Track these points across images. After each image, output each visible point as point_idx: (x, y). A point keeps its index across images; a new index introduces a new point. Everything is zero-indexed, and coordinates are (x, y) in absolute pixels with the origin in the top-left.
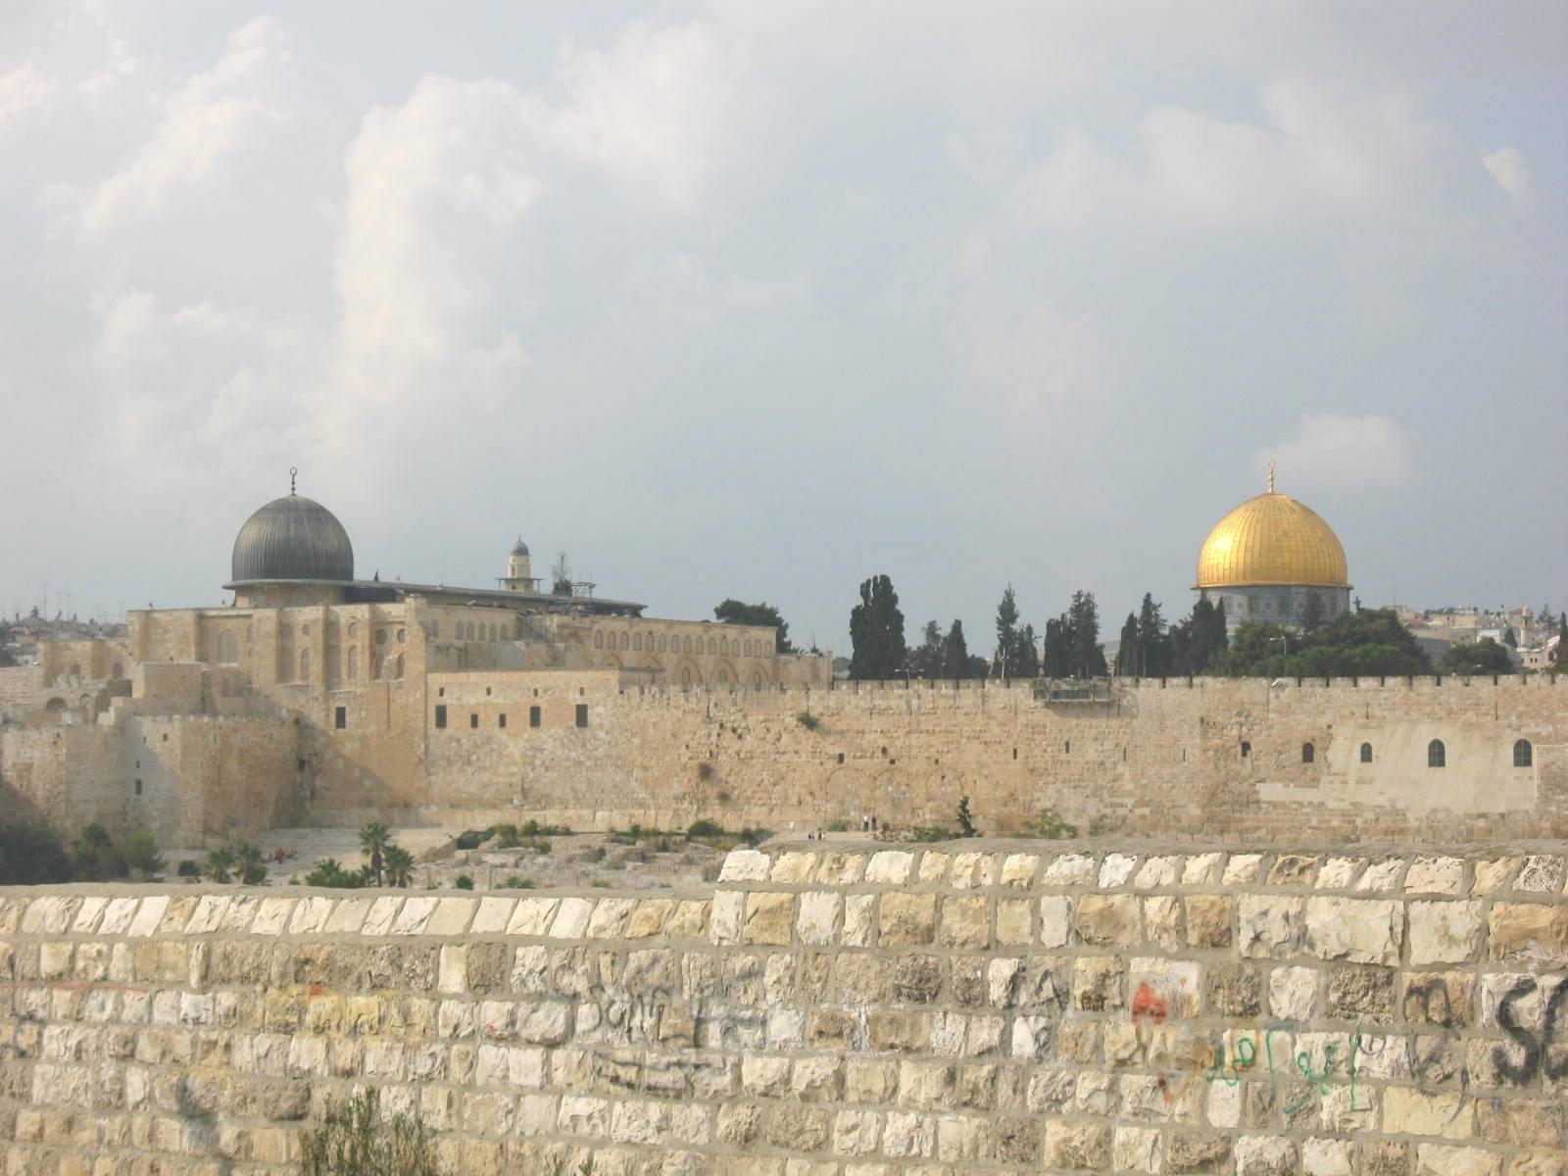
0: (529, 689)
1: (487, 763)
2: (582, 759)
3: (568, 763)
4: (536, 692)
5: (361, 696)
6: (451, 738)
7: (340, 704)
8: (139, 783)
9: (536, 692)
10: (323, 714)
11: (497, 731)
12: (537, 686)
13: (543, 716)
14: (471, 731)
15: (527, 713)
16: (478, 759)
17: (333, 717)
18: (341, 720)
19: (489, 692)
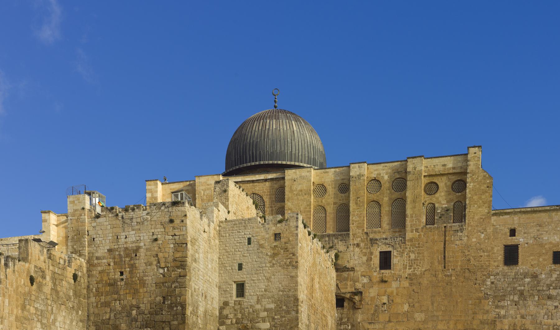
6: (525, 275)
7: (385, 249)
10: (365, 259)
17: (376, 260)
18: (386, 261)
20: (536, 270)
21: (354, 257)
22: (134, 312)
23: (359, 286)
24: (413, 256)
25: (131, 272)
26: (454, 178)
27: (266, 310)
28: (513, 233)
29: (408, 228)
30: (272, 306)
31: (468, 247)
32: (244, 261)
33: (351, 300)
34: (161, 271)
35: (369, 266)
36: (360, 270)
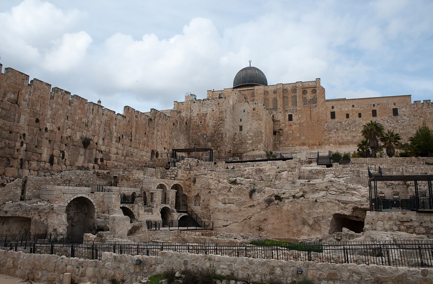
0: (371, 105)
1: (354, 130)
2: (397, 126)
3: (391, 128)
4: (374, 105)
5: (299, 110)
6: (338, 122)
8: (241, 128)
9: (374, 105)
11: (357, 118)
12: (374, 103)
13: (378, 113)
14: (346, 119)
15: (371, 112)
16: (350, 128)
18: (290, 118)
19: (353, 106)
20: (341, 120)
21: (280, 117)
22: (205, 136)
23: (281, 127)
24: (300, 116)
25: (204, 122)
26: (312, 89)
27: (250, 136)
28: (333, 107)
29: (298, 106)
30: (252, 134)
31: (318, 112)
32: (242, 118)
33: (279, 132)
34: (214, 121)
35: (285, 120)
36: (282, 121)
